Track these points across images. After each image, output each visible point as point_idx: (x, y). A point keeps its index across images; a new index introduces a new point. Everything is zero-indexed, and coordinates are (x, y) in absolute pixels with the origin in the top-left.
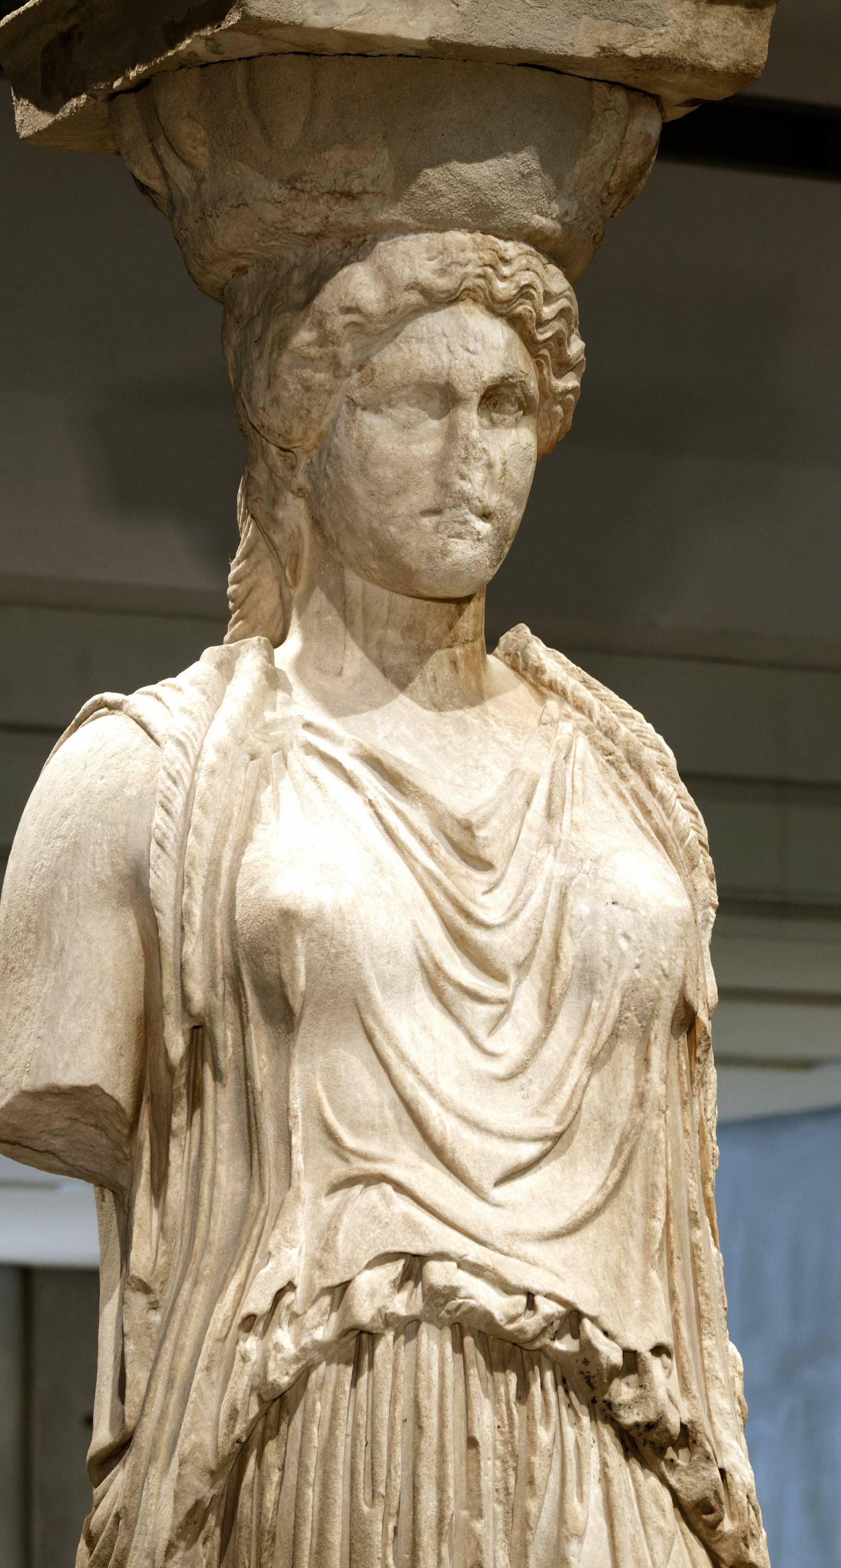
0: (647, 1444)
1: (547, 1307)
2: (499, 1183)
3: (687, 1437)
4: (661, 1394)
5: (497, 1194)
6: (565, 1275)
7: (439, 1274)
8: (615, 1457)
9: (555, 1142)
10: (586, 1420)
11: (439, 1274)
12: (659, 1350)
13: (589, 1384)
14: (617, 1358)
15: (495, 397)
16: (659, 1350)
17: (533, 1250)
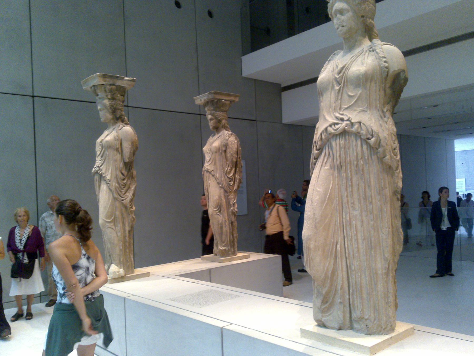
0: (213, 176)
9: (210, 160)
13: (210, 173)
15: (211, 119)
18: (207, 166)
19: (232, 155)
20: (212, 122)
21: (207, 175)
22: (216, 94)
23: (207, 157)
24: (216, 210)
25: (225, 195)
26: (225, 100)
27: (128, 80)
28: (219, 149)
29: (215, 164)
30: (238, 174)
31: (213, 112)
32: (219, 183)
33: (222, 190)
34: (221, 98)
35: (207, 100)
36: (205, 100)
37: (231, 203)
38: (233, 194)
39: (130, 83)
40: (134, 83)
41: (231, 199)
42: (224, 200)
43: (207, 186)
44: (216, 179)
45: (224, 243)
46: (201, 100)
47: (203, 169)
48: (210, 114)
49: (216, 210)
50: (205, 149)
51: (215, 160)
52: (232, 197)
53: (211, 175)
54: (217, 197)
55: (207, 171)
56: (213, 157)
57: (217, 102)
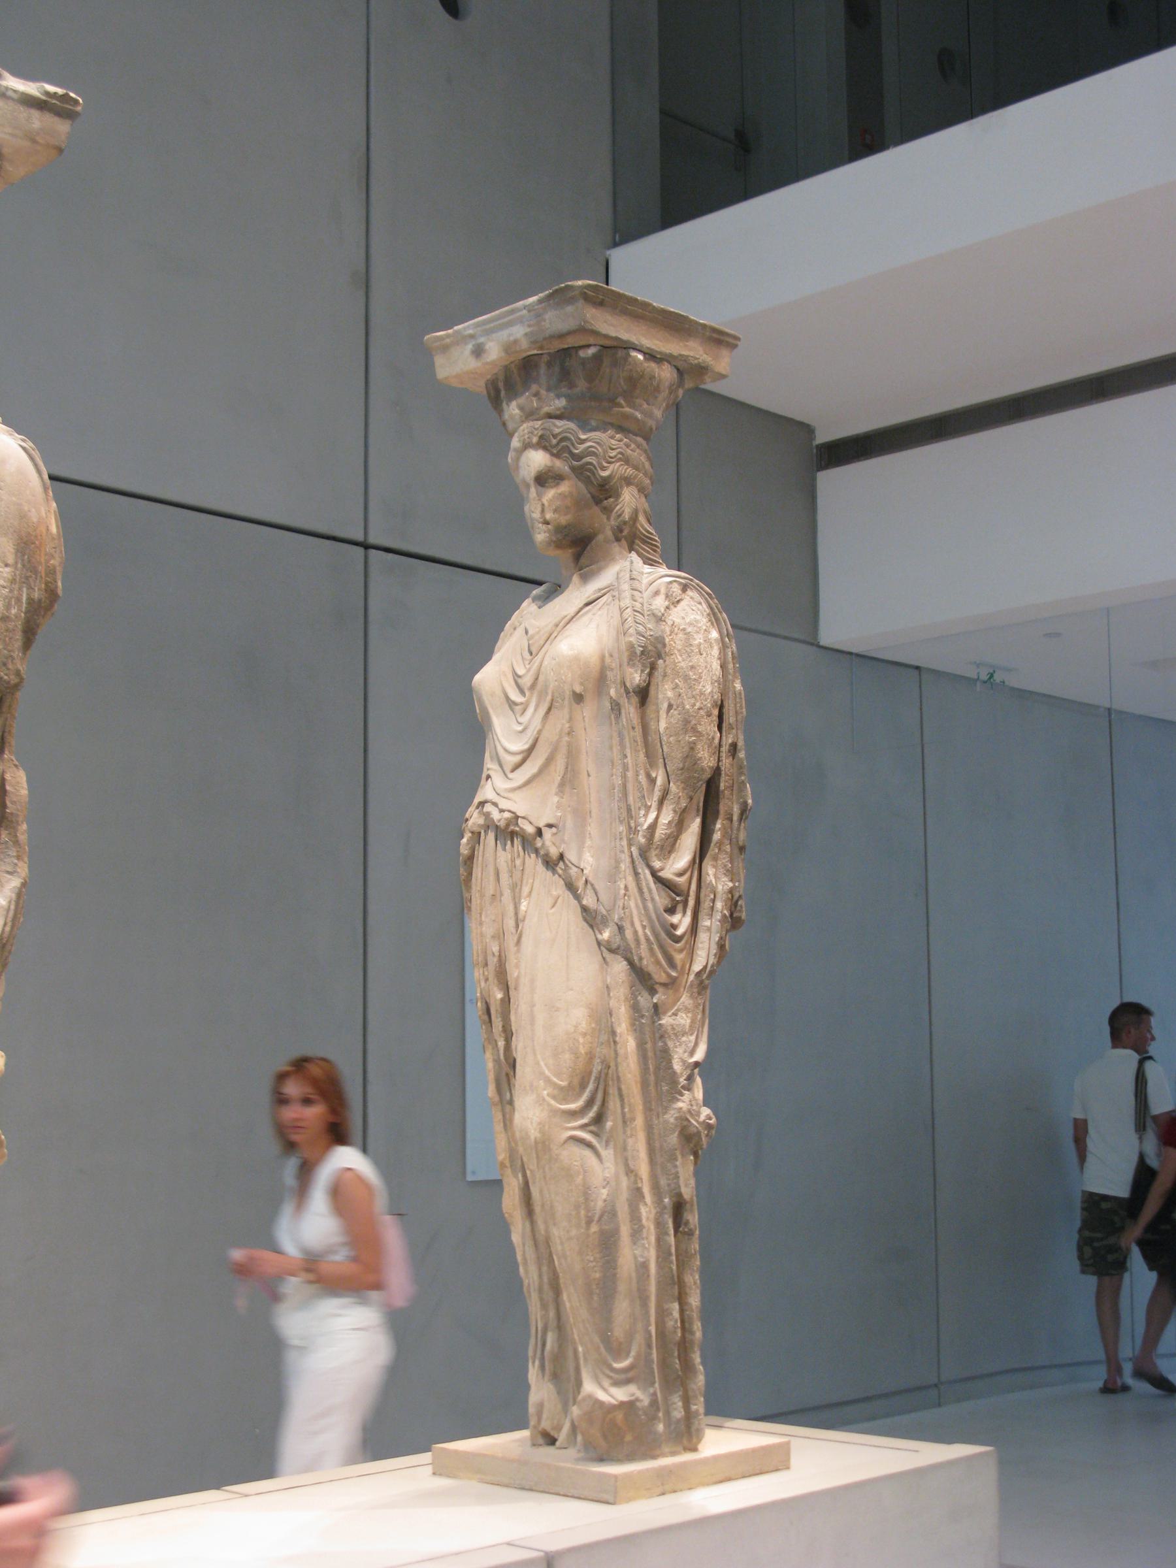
0: (552, 863)
1: (507, 815)
2: (513, 771)
3: (561, 857)
4: (548, 843)
5: (510, 775)
6: (520, 804)
7: (488, 808)
8: (540, 867)
9: (528, 753)
10: (533, 856)
11: (488, 808)
12: (550, 826)
14: (530, 830)
15: (543, 479)
16: (550, 826)
17: (510, 795)
18: (503, 792)
19: (688, 725)
20: (550, 493)
21: (504, 857)
22: (601, 304)
23: (508, 735)
24: (573, 1114)
25: (635, 1008)
26: (651, 356)
27: (29, 102)
28: (601, 680)
29: (569, 781)
30: (724, 859)
31: (561, 426)
32: (591, 918)
33: (619, 967)
34: (625, 336)
35: (526, 348)
36: (508, 348)
37: (677, 1066)
38: (685, 999)
39: (37, 120)
40: (63, 127)
41: (679, 1033)
42: (629, 1044)
43: (500, 936)
44: (570, 886)
45: (619, 1351)
46: (478, 352)
47: (475, 819)
48: (543, 443)
49: (573, 1114)
50: (489, 678)
51: (572, 756)
52: (684, 1020)
53: (533, 863)
54: (575, 1018)
55: (508, 833)
56: (551, 733)
57: (597, 358)
